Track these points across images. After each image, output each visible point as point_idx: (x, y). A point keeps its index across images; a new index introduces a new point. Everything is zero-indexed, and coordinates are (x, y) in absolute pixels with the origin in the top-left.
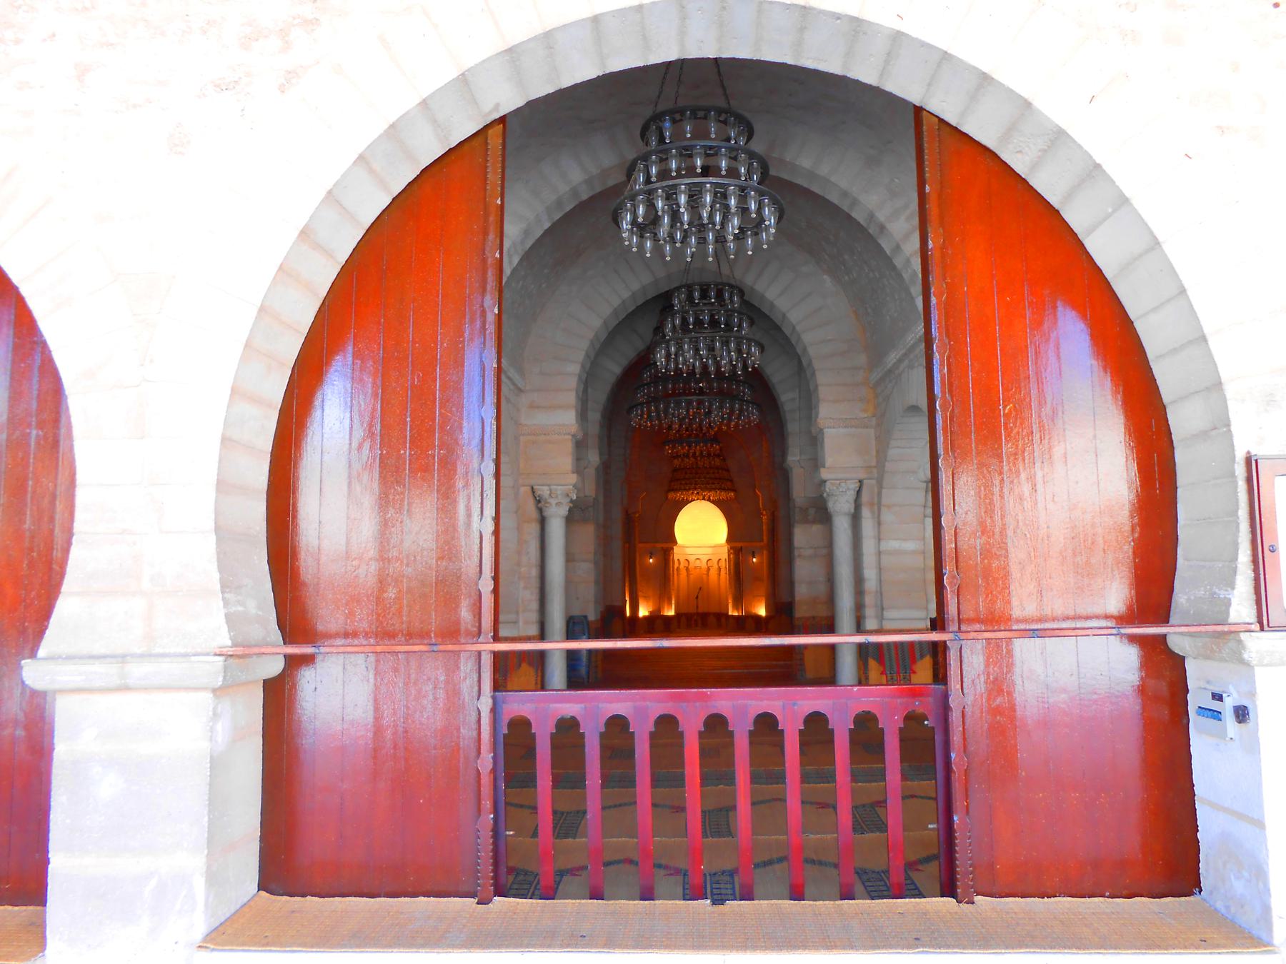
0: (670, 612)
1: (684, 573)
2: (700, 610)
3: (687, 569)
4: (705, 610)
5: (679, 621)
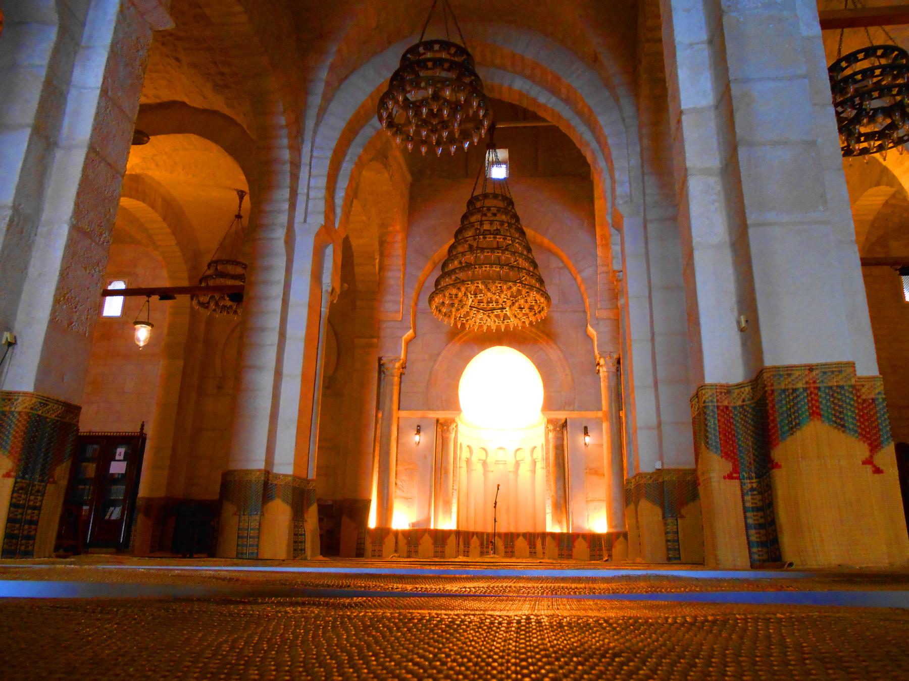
0: (447, 522)
1: (478, 468)
2: (503, 528)
3: (484, 464)
4: (512, 530)
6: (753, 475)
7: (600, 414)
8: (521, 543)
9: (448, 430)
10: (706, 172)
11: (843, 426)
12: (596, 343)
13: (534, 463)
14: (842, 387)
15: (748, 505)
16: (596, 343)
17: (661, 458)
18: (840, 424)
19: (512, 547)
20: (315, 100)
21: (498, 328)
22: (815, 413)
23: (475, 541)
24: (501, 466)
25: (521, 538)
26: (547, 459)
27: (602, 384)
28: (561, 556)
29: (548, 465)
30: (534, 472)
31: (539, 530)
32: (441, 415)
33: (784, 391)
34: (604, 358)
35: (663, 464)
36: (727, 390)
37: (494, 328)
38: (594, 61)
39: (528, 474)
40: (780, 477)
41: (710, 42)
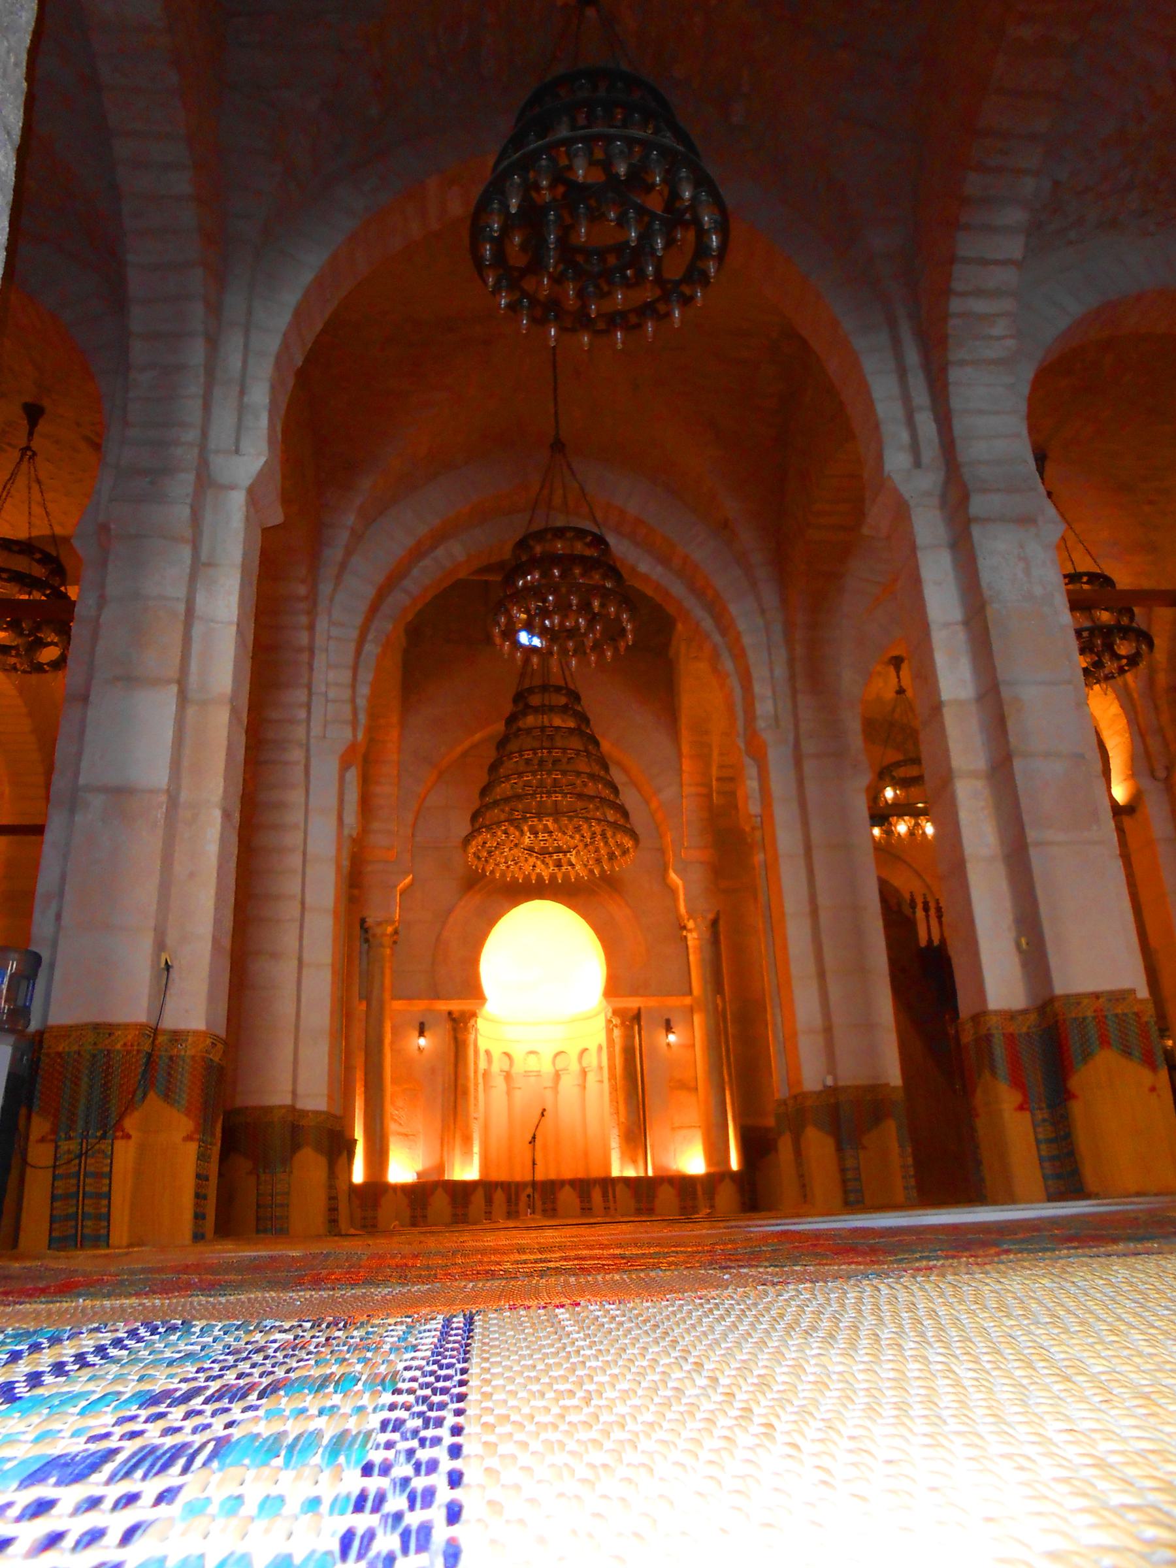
0: (466, 1170)
1: (499, 1083)
2: (540, 1176)
3: (508, 1076)
5: (489, 1201)
6: (1044, 1105)
7: (688, 1001)
8: (567, 1197)
9: (466, 1029)
10: (974, 774)
11: (1130, 1054)
12: (682, 897)
13: (584, 1073)
14: (1125, 1015)
15: (1041, 1137)
16: (682, 897)
17: (832, 1069)
18: (1127, 1052)
19: (554, 1201)
20: (334, 554)
21: (553, 877)
22: (1105, 1042)
23: (499, 1196)
24: (533, 1079)
25: (567, 1188)
26: (612, 1068)
27: (692, 958)
28: (638, 1212)
29: (612, 1076)
30: (584, 1088)
31: (596, 1173)
32: (455, 1006)
33: (1075, 1019)
34: (695, 921)
35: (835, 1079)
36: (1010, 1016)
37: (546, 875)
38: (724, 528)
39: (576, 1090)
40: (1077, 1108)
41: (966, 623)
